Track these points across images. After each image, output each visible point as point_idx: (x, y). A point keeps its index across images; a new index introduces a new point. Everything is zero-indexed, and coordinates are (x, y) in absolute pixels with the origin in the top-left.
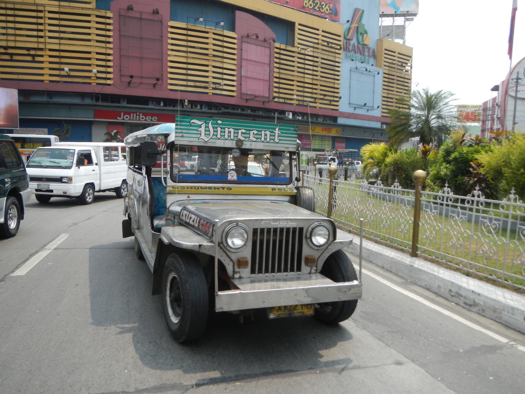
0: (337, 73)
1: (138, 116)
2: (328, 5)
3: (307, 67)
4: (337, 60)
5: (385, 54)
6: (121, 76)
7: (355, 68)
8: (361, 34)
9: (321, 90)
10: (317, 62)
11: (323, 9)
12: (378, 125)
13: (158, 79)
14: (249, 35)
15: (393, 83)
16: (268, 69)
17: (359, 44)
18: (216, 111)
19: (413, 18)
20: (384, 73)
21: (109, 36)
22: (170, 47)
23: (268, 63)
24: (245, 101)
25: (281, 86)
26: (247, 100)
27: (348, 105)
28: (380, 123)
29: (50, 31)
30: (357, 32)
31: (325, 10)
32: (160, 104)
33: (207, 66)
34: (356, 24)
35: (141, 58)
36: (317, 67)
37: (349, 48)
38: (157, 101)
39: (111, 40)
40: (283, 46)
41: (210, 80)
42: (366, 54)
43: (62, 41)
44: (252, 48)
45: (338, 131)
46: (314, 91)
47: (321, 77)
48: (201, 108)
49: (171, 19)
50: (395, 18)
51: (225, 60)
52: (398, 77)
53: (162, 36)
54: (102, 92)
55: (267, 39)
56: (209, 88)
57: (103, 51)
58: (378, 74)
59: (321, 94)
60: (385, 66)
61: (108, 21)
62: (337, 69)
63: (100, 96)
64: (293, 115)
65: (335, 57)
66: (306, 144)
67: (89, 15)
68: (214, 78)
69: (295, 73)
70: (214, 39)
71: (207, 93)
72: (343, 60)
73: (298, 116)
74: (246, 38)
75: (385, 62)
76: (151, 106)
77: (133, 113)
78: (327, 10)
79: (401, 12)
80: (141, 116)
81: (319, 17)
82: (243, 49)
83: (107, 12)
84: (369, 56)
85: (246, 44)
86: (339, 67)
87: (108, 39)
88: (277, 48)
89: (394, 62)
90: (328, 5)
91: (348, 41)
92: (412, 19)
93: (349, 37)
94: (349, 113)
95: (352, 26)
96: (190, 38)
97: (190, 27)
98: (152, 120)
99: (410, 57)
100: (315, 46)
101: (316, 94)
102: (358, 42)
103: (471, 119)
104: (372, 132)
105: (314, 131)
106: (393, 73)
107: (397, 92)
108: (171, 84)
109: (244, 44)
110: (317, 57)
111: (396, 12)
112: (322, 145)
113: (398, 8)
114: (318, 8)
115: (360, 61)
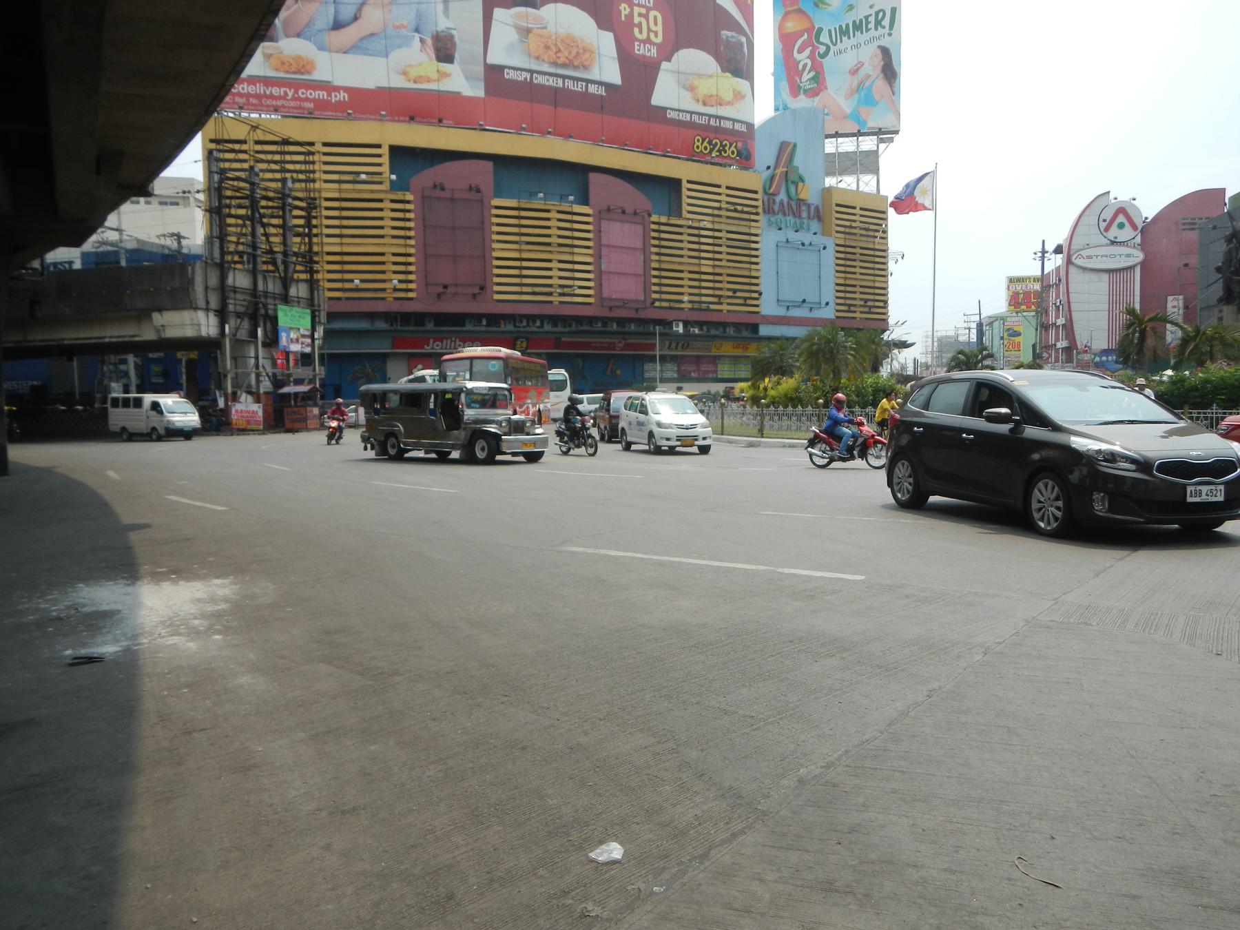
0: (754, 253)
1: (453, 343)
2: (735, 144)
3: (703, 247)
4: (753, 231)
5: (837, 212)
6: (427, 285)
7: (785, 240)
8: (793, 182)
10: (720, 238)
11: (725, 152)
13: (482, 288)
14: (611, 208)
15: (855, 260)
16: (642, 257)
17: (790, 201)
18: (567, 329)
19: (893, 138)
20: (837, 245)
21: (409, 229)
22: (495, 237)
23: (642, 247)
26: (611, 308)
29: (328, 227)
30: (787, 181)
31: (729, 152)
32: (481, 322)
33: (550, 261)
36: (720, 246)
37: (772, 208)
38: (477, 318)
39: (412, 233)
42: (804, 215)
43: (345, 240)
46: (717, 285)
47: (729, 261)
48: (542, 326)
49: (498, 195)
50: (860, 138)
51: (576, 250)
52: (861, 248)
53: (483, 222)
54: (401, 311)
55: (638, 211)
56: (555, 294)
57: (402, 250)
59: (729, 290)
60: (837, 232)
61: (408, 206)
62: (753, 246)
64: (685, 326)
65: (750, 227)
66: (708, 372)
67: (381, 201)
70: (559, 220)
72: (763, 230)
73: (692, 327)
74: (605, 213)
75: (837, 225)
76: (469, 327)
77: (447, 339)
78: (733, 153)
79: (870, 128)
81: (721, 165)
82: (602, 230)
83: (406, 193)
84: (809, 217)
85: (607, 222)
86: (757, 242)
87: (408, 233)
88: (654, 223)
89: (854, 224)
90: (735, 144)
91: (771, 197)
92: (891, 140)
93: (774, 190)
95: (776, 171)
99: (884, 213)
100: (716, 212)
106: (853, 244)
107: (862, 274)
109: (603, 222)
110: (720, 231)
113: (865, 122)
114: (719, 151)
115: (793, 227)
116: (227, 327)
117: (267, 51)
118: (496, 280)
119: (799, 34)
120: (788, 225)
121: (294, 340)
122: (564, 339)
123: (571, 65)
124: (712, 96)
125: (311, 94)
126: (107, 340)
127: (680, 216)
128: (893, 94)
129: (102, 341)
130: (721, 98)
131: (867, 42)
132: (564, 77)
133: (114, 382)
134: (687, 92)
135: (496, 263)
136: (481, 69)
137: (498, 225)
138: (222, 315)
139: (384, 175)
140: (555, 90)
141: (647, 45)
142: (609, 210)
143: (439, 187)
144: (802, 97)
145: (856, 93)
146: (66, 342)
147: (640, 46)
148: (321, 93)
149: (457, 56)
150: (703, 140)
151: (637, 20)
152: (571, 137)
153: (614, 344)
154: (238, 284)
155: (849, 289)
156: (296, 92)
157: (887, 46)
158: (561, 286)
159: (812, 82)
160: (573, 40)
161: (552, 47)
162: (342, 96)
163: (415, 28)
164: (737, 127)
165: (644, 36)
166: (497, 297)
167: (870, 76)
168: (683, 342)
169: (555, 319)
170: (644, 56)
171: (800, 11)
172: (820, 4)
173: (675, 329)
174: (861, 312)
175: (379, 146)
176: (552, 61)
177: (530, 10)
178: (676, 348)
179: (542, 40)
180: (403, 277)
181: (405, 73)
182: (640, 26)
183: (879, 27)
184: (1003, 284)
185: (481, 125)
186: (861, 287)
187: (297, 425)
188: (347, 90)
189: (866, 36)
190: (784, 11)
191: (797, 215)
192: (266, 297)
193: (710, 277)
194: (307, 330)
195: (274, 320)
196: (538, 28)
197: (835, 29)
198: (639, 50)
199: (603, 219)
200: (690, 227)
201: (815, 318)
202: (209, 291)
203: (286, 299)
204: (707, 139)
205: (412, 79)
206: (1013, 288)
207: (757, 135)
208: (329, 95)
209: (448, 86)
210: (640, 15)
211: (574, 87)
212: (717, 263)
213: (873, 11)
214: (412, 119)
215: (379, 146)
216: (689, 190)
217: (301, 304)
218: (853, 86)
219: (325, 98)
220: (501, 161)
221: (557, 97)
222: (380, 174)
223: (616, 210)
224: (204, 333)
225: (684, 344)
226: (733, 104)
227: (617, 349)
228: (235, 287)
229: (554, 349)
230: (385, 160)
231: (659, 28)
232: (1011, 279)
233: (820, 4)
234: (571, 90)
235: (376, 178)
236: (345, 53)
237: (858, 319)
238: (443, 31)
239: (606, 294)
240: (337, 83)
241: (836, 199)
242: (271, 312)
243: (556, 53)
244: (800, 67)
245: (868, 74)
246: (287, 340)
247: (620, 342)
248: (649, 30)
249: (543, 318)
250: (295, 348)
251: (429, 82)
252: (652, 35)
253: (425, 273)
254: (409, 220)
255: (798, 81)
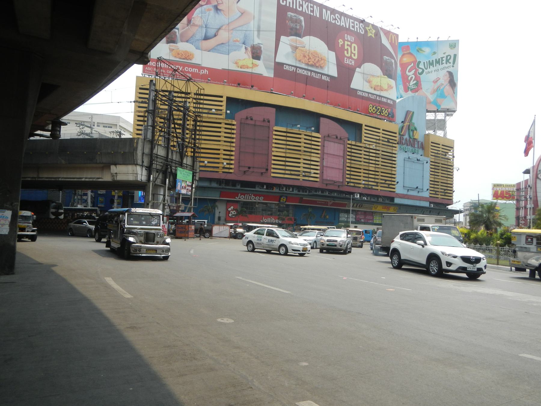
0: (394, 162)
1: (250, 196)
2: (387, 110)
4: (394, 152)
6: (239, 166)
7: (408, 158)
8: (412, 130)
9: (382, 176)
10: (379, 154)
11: (383, 113)
12: (426, 204)
14: (330, 135)
15: (439, 170)
16: (343, 160)
17: (410, 139)
21: (233, 138)
22: (274, 145)
23: (343, 155)
24: (325, 185)
25: (352, 173)
26: (327, 184)
27: (403, 188)
28: (429, 203)
30: (409, 129)
31: (384, 113)
32: (264, 187)
33: (299, 159)
34: (407, 123)
35: (254, 154)
36: (379, 158)
38: (262, 184)
39: (234, 140)
40: (353, 143)
41: (301, 169)
42: (416, 146)
44: (332, 144)
45: (395, 209)
46: (376, 177)
47: (382, 165)
48: (293, 191)
49: (276, 125)
50: (437, 113)
51: (312, 155)
53: (269, 138)
56: (301, 176)
57: (229, 148)
58: (427, 162)
61: (233, 127)
62: (394, 159)
63: (224, 181)
64: (360, 196)
65: (392, 150)
66: (369, 220)
67: (220, 123)
68: (304, 168)
69: (362, 163)
71: (299, 179)
74: (327, 137)
75: (431, 152)
76: (257, 189)
78: (386, 114)
79: (442, 109)
80: (252, 196)
81: (380, 119)
82: (325, 145)
83: (233, 120)
84: (418, 148)
85: (327, 142)
86: (395, 157)
89: (439, 152)
90: (387, 110)
91: (402, 137)
92: (452, 115)
94: (403, 194)
95: (405, 124)
96: (288, 139)
97: (288, 131)
98: (259, 200)
99: (452, 148)
100: (378, 141)
101: (378, 179)
102: (410, 137)
103: (505, 197)
104: (422, 210)
105: (376, 209)
106: (438, 162)
107: (442, 176)
108: (274, 173)
110: (379, 150)
111: (438, 110)
112: (381, 220)
113: (440, 106)
114: (380, 112)
116: (152, 176)
117: (171, 47)
118: (273, 166)
119: (409, 64)
120: (409, 150)
121: (184, 188)
122: (304, 198)
123: (315, 65)
124: (378, 86)
125: (190, 70)
126: (83, 180)
127: (361, 142)
128: (454, 93)
129: (80, 180)
130: (382, 87)
131: (442, 69)
132: (311, 71)
133: (80, 205)
134: (367, 83)
135: (273, 158)
136: (273, 64)
137: (276, 139)
138: (149, 169)
139: (223, 111)
140: (307, 77)
141: (350, 60)
142: (329, 136)
143: (250, 119)
144: (410, 92)
145: (436, 91)
146: (60, 179)
147: (347, 59)
148: (195, 70)
149: (262, 56)
150: (373, 107)
151: (346, 47)
152: (313, 99)
153: (328, 202)
154: (159, 154)
155: (436, 183)
156: (184, 68)
157: (451, 71)
158: (304, 172)
159: (415, 86)
160: (317, 53)
161: (307, 56)
162: (206, 72)
163: (243, 42)
164: (389, 101)
165: (349, 55)
166: (273, 175)
167: (443, 84)
168: (360, 204)
169: (300, 188)
170: (349, 64)
171: (410, 53)
172: (420, 51)
173: (355, 197)
174: (441, 195)
175: (222, 97)
176: (306, 63)
177: (298, 38)
178: (356, 206)
179: (303, 53)
180: (228, 162)
181: (236, 63)
182: (347, 50)
183: (448, 63)
184: (491, 187)
185: (272, 90)
186: (442, 183)
187: (183, 235)
188: (208, 69)
189: (441, 66)
190: (402, 54)
191: (413, 146)
192: (172, 162)
193: (373, 173)
194: (190, 182)
195: (175, 176)
196: (301, 47)
197: (427, 62)
198: (346, 61)
199: (326, 140)
200: (365, 148)
201: (420, 196)
202: (144, 155)
203: (181, 165)
204: (375, 106)
205: (240, 66)
206: (495, 189)
207: (397, 106)
208: (199, 71)
209: (256, 71)
210: (348, 45)
211: (315, 76)
212: (377, 166)
213: (445, 56)
214: (239, 84)
215: (222, 97)
216: (366, 129)
217: (188, 168)
218: (435, 89)
219: (197, 72)
220: (280, 109)
221: (307, 80)
222: (221, 110)
223: (332, 137)
224: (139, 179)
225: (360, 204)
226: (387, 91)
227: (329, 205)
228: (157, 155)
229: (299, 203)
230: (224, 103)
231: (356, 52)
232: (494, 185)
233: (420, 51)
234: (314, 77)
235: (219, 112)
236: (208, 51)
237: (439, 198)
238: (256, 45)
239: (325, 177)
240: (204, 65)
241: (431, 140)
242: (173, 171)
243: (308, 59)
244: (409, 78)
245: (442, 83)
246: (180, 187)
247: (331, 202)
248: (351, 52)
249: (293, 187)
250: (184, 191)
251: (248, 68)
252: (353, 55)
253: (239, 161)
254: (233, 134)
255: (408, 85)
